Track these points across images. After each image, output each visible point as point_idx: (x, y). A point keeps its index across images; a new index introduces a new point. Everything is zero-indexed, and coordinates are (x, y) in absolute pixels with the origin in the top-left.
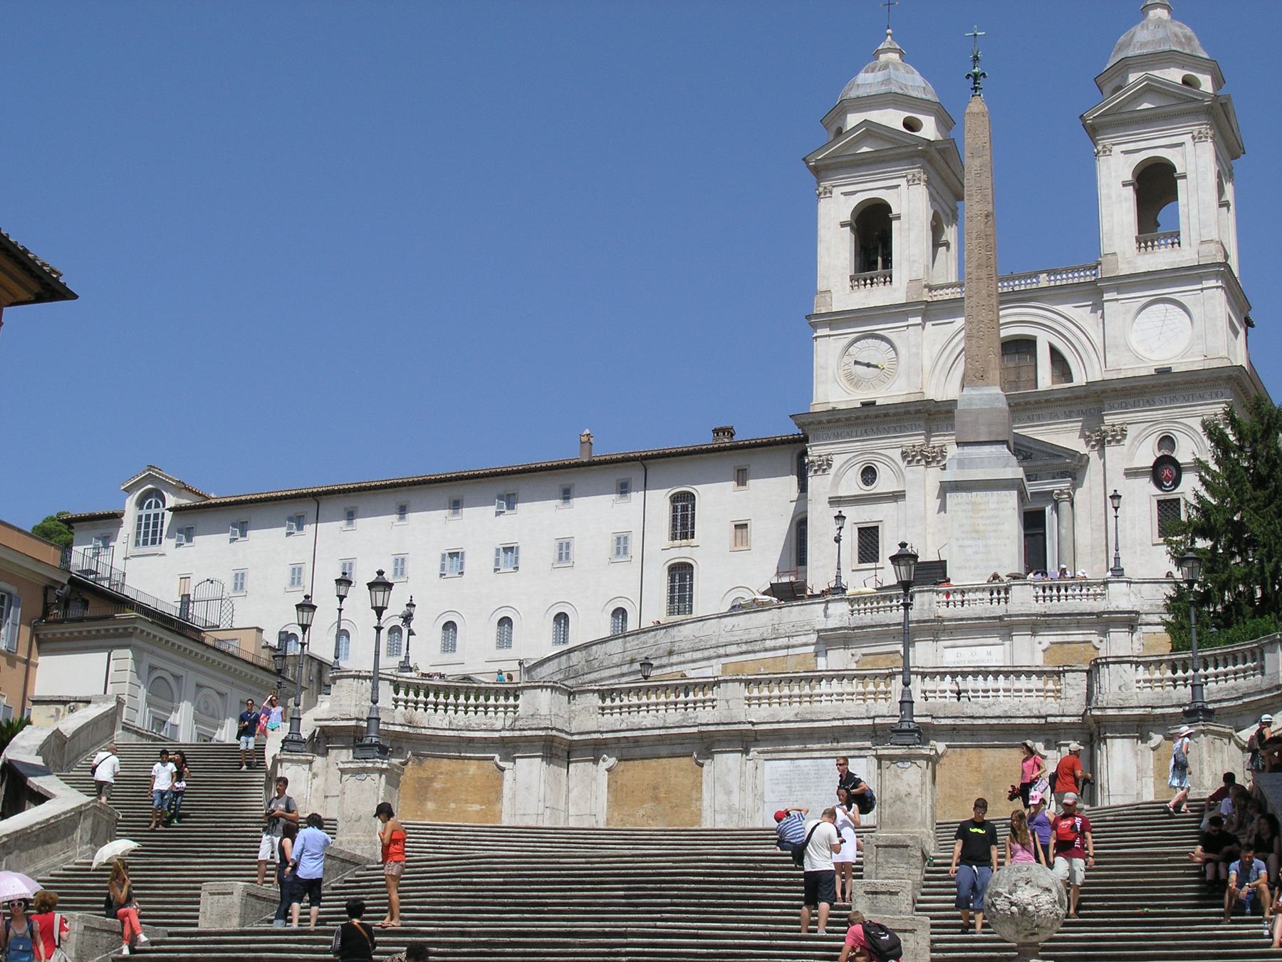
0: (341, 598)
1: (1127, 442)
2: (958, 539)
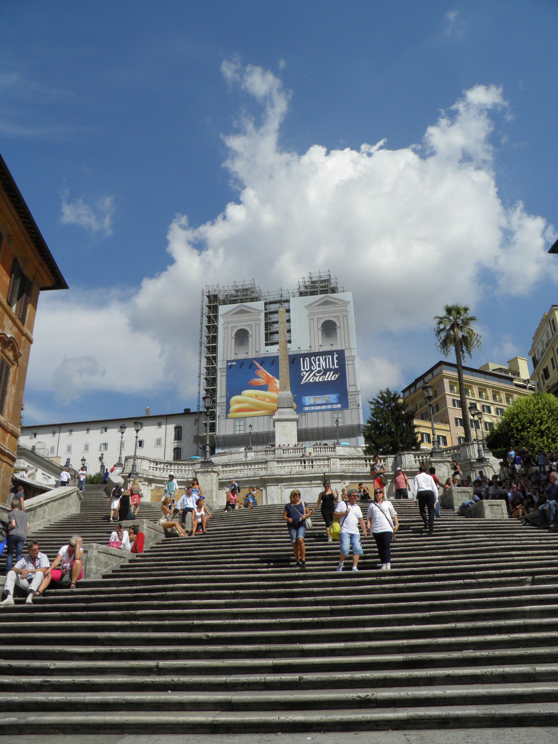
0: (122, 433)
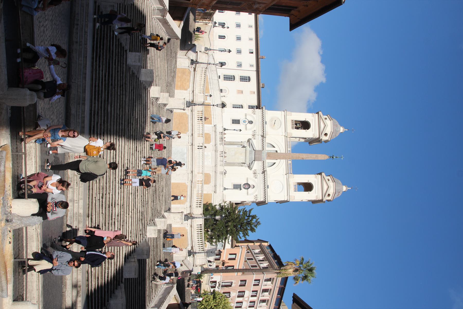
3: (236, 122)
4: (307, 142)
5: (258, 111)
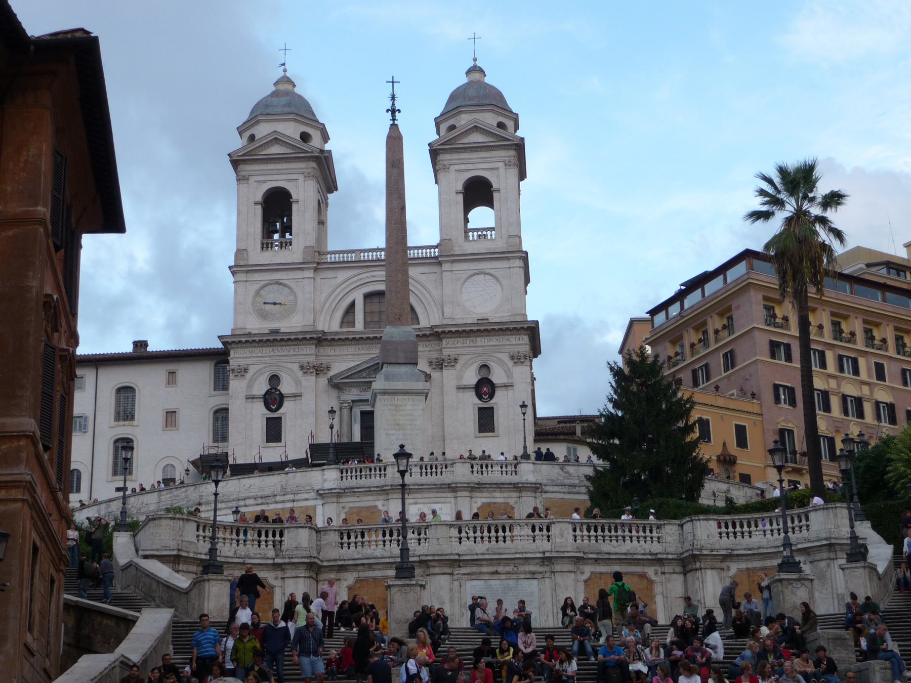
1: (458, 366)
2: (385, 430)
3: (274, 431)
4: (326, 199)
5: (237, 358)
